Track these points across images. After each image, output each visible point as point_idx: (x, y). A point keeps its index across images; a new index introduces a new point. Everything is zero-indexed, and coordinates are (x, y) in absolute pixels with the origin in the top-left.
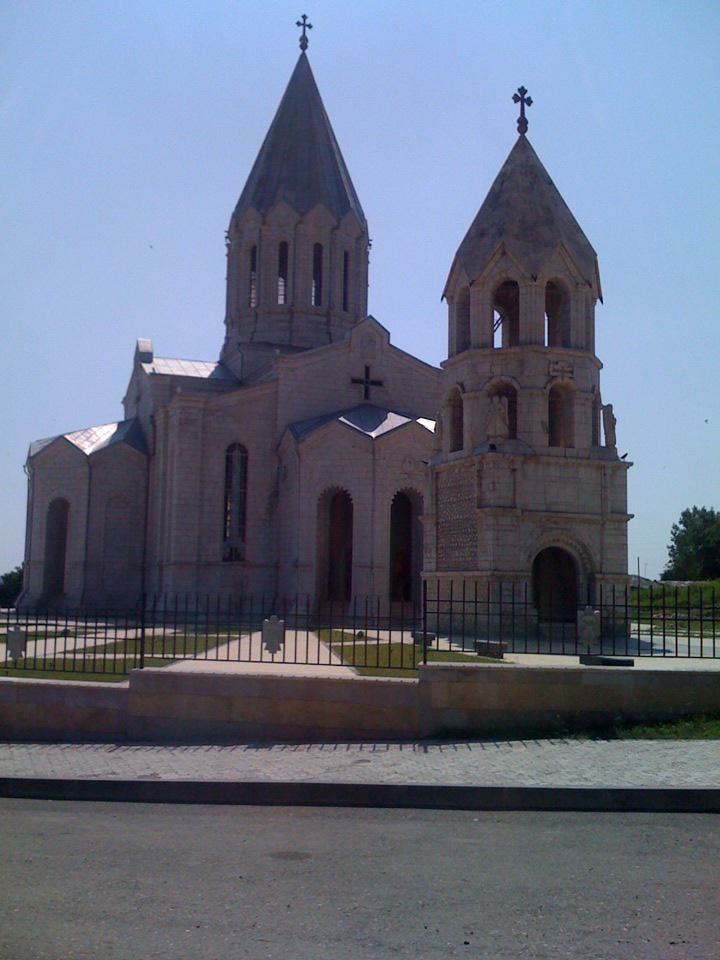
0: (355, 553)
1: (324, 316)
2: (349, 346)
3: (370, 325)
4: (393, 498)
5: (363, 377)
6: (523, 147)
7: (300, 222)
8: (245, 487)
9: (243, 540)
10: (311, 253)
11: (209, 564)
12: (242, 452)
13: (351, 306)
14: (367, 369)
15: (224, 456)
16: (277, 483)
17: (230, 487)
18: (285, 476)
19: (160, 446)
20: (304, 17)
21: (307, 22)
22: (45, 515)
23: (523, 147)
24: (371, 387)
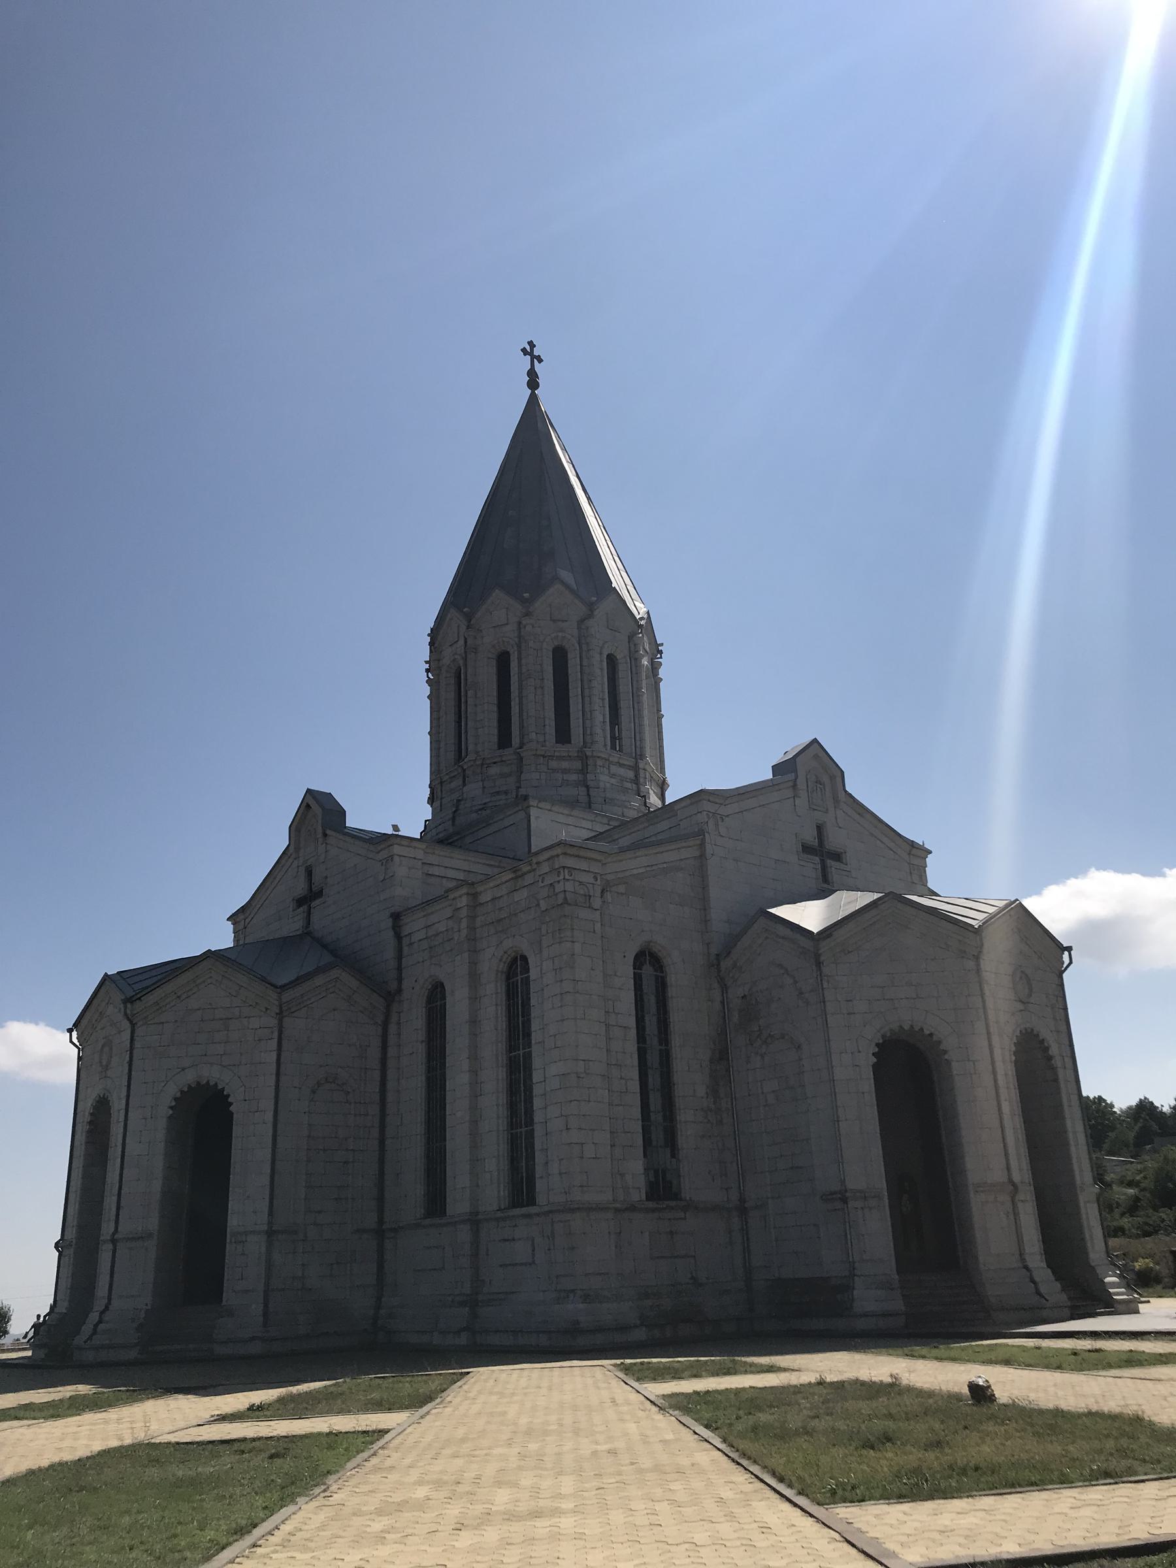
1: (629, 767)
2: (795, 786)
3: (816, 757)
5: (816, 844)
7: (590, 615)
8: (667, 1045)
9: (673, 1156)
11: (632, 1208)
12: (656, 971)
14: (820, 828)
15: (630, 971)
17: (645, 1042)
20: (531, 344)
21: (536, 353)
22: (162, 1123)
24: (829, 862)
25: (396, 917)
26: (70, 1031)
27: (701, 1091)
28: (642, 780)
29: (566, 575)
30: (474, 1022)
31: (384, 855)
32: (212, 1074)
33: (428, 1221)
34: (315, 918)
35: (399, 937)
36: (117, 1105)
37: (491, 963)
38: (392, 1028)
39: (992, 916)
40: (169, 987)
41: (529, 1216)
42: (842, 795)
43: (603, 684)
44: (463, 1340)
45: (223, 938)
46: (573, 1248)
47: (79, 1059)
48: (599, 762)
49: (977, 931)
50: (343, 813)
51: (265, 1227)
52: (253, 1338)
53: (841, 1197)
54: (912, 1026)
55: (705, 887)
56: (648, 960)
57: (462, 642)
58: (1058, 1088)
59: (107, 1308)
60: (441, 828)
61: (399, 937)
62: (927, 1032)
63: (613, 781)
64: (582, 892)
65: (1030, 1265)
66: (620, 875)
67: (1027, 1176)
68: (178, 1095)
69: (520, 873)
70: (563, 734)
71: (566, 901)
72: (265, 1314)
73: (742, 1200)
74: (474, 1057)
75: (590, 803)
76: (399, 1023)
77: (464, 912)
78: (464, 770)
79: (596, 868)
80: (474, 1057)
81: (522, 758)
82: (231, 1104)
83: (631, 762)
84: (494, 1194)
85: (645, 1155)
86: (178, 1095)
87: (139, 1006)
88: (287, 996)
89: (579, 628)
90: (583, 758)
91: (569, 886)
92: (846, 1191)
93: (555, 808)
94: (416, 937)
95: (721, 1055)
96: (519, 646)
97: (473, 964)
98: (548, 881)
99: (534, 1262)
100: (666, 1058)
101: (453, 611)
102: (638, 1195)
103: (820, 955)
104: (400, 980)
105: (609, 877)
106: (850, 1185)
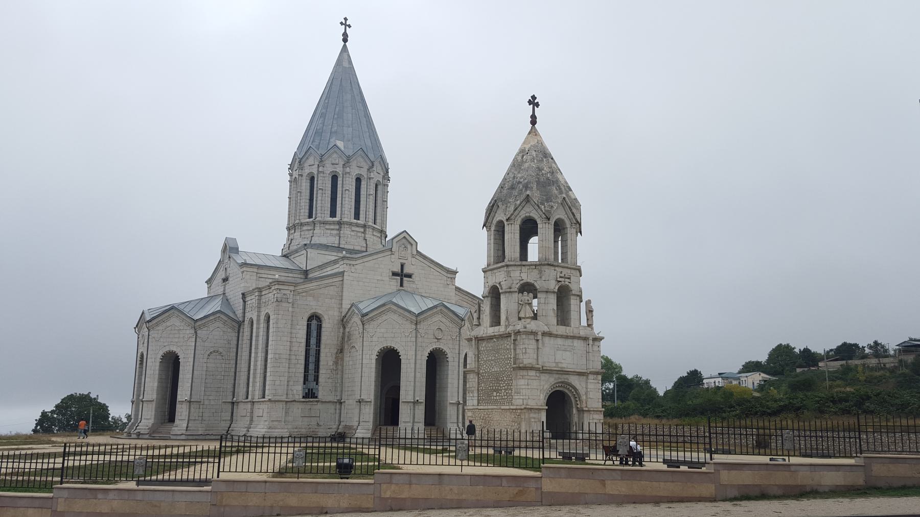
0: (402, 392)
6: (533, 132)
10: (354, 184)
11: (294, 401)
13: (378, 221)
14: (402, 266)
15: (305, 323)
19: (251, 314)
22: (158, 364)
23: (533, 132)
24: (405, 279)
25: (243, 294)
27: (331, 363)
30: (257, 336)
32: (174, 349)
35: (245, 302)
37: (262, 317)
56: (315, 320)
61: (245, 302)
70: (333, 214)
74: (257, 348)
79: (292, 288)
84: (258, 394)
87: (151, 324)
88: (198, 324)
91: (279, 296)
97: (259, 316)
100: (318, 353)
102: (299, 396)
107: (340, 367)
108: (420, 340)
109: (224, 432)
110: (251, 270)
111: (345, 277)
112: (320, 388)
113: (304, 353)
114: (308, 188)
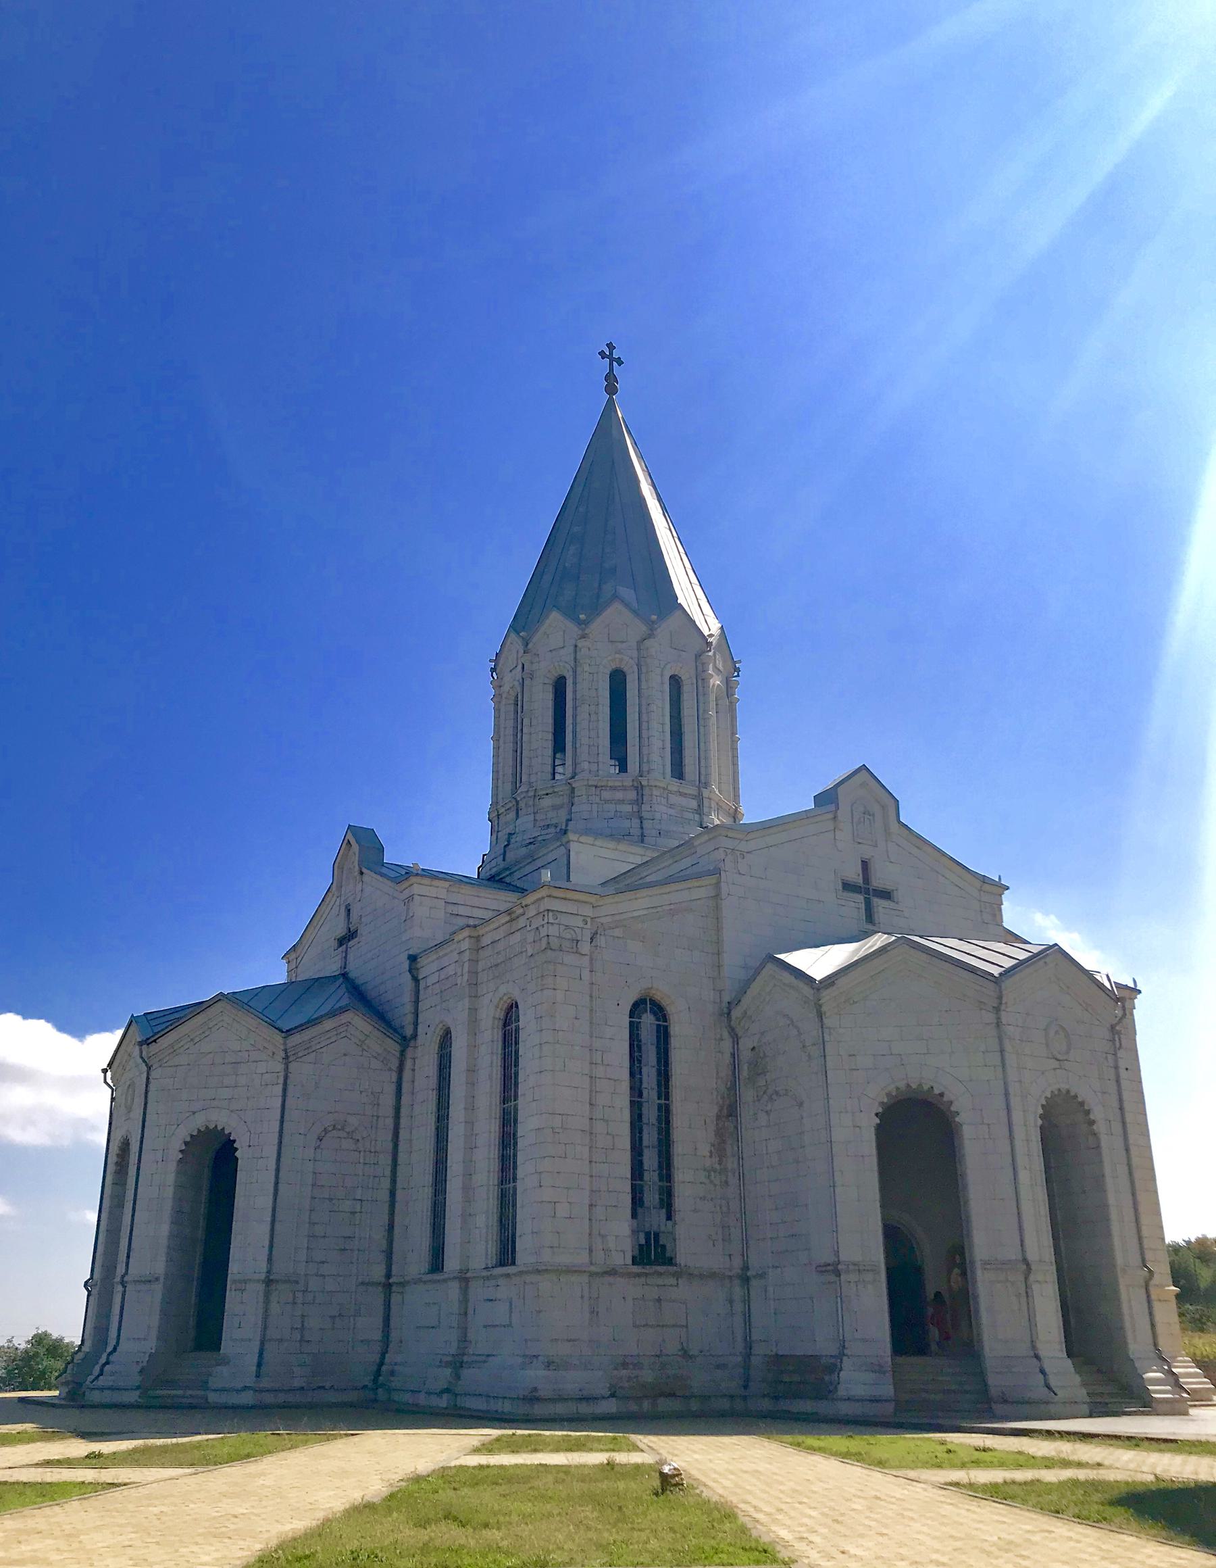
1: (694, 797)
2: (835, 818)
3: (864, 785)
4: (1041, 1111)
5: (860, 881)
7: (651, 636)
8: (667, 1098)
9: (669, 1218)
11: (612, 1272)
12: (658, 1020)
14: (865, 865)
15: (626, 1020)
16: (733, 1087)
17: (641, 1095)
18: (758, 1069)
22: (172, 1167)
24: (876, 901)
25: (413, 959)
26: (105, 1071)
27: (704, 1149)
28: (706, 810)
29: (626, 593)
30: (472, 1070)
31: (407, 893)
32: (222, 1119)
33: (430, 1277)
34: (351, 957)
35: (416, 980)
36: (134, 1147)
38: (407, 1075)
39: (1021, 963)
40: (183, 1029)
41: (508, 1275)
42: (894, 827)
43: (663, 709)
44: (443, 1402)
45: (278, 975)
46: (540, 1312)
47: (113, 1099)
48: (655, 792)
49: (996, 980)
50: (381, 850)
51: (263, 1276)
52: (245, 1388)
53: (833, 1269)
54: (920, 1085)
55: (719, 929)
57: (520, 667)
58: (1100, 1154)
59: (115, 1349)
60: (494, 863)
61: (416, 980)
62: (937, 1091)
63: (671, 812)
64: (569, 936)
65: (1042, 1354)
66: (617, 918)
67: (1049, 1255)
68: (188, 1139)
69: (513, 916)
71: (549, 947)
72: (259, 1365)
73: (746, 1268)
74: (471, 1107)
75: (643, 835)
76: (413, 1070)
77: (467, 956)
78: (517, 802)
79: (588, 911)
80: (471, 1107)
81: (573, 789)
82: (236, 1149)
83: (696, 793)
84: (483, 1249)
85: (634, 1215)
86: (188, 1139)
89: (639, 650)
90: (639, 789)
91: (553, 931)
92: (839, 1262)
93: (598, 843)
94: (430, 981)
95: (730, 1111)
96: (575, 672)
97: (473, 1010)
98: (534, 926)
99: (510, 1325)
100: (665, 1113)
101: (513, 635)
103: (820, 1006)
104: (416, 1024)
105: (603, 920)
106: (842, 1258)
107: (731, 1163)
108: (1011, 1059)
109: (367, 1381)
110: (433, 892)
111: (724, 889)
112: (681, 1231)
113: (627, 1115)
114: (550, 704)
